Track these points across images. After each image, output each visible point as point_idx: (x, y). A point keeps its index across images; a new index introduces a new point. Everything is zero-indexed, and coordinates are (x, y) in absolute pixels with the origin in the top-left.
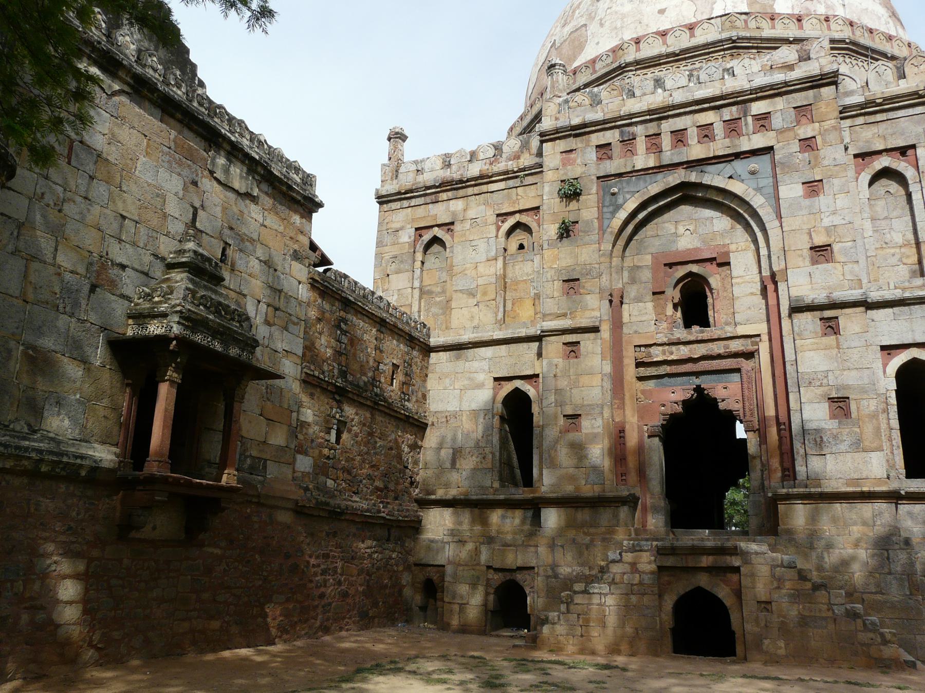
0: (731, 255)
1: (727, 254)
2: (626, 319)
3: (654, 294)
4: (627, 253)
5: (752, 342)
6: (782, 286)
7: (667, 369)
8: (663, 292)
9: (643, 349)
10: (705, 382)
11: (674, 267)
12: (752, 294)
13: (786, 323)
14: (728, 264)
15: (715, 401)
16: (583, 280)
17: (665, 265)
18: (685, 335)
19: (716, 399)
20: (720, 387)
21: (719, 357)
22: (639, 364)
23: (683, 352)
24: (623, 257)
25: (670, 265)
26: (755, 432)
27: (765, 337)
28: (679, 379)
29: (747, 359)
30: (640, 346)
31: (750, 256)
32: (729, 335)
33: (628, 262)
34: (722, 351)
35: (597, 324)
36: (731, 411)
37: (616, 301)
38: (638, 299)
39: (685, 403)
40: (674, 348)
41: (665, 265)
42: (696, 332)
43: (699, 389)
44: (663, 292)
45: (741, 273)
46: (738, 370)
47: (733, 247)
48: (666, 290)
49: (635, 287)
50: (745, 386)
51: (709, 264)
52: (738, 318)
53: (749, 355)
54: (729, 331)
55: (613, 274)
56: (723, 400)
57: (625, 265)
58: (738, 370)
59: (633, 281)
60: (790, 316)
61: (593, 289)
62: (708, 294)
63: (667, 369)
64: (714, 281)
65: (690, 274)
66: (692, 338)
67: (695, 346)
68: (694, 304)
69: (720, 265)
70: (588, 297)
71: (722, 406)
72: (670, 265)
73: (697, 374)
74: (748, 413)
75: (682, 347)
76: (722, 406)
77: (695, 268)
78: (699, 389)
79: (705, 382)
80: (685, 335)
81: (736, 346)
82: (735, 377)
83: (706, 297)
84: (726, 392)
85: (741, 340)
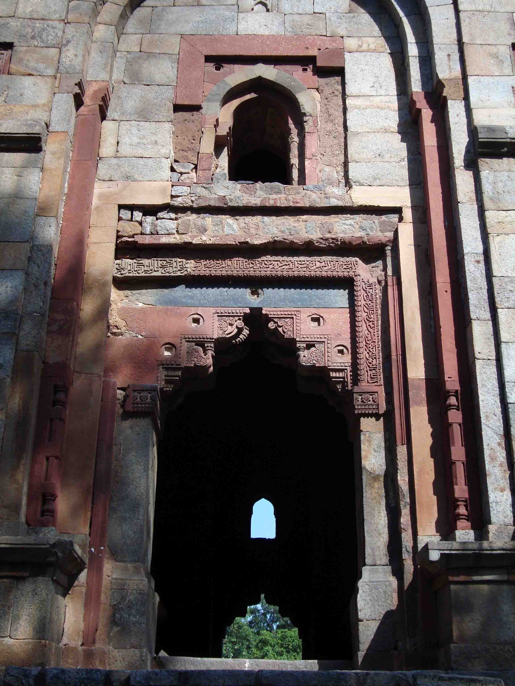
0: (347, 56)
1: (340, 53)
2: (107, 149)
3: (178, 108)
4: (131, 25)
5: (382, 223)
6: (455, 111)
7: (191, 267)
8: (197, 108)
9: (138, 215)
10: (273, 302)
11: (227, 68)
12: (386, 131)
13: (464, 180)
14: (339, 72)
15: (290, 347)
16: (20, 48)
17: (208, 59)
18: (238, 193)
19: (293, 341)
20: (305, 315)
21: (309, 249)
22: (125, 249)
23: (231, 230)
24: (120, 33)
25: (219, 61)
26: (377, 416)
27: (408, 214)
28: (212, 293)
29: (367, 261)
30: (132, 208)
31: (385, 63)
32: (334, 202)
33: (131, 43)
34: (315, 235)
35: (37, 129)
36: (324, 371)
37: (94, 107)
38: (144, 115)
39: (223, 346)
40: (209, 220)
41: (208, 59)
42: (260, 193)
43: (255, 319)
44: (197, 108)
45: (366, 90)
46: (347, 283)
47: (351, 43)
48: (204, 105)
49: (138, 91)
50: (362, 315)
51: (300, 68)
52: (355, 172)
53: (371, 252)
54: (336, 196)
55: (93, 54)
56: (310, 346)
57: (122, 47)
58: (347, 283)
59: (134, 77)
60: (471, 164)
61: (41, 66)
62: (294, 131)
63: (191, 267)
64: (309, 101)
65: (258, 84)
66: (255, 201)
67: (258, 219)
68: (262, 138)
69: (323, 72)
70: (28, 81)
71: (306, 357)
72: (219, 61)
73: (256, 284)
74: (365, 375)
75: (228, 220)
76: (306, 357)
77: (269, 72)
78: (255, 319)
79: (273, 302)
80: (238, 193)
81: (346, 228)
82: (340, 296)
83: (288, 132)
84: (320, 328)
85: (358, 218)
